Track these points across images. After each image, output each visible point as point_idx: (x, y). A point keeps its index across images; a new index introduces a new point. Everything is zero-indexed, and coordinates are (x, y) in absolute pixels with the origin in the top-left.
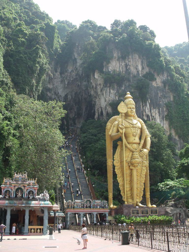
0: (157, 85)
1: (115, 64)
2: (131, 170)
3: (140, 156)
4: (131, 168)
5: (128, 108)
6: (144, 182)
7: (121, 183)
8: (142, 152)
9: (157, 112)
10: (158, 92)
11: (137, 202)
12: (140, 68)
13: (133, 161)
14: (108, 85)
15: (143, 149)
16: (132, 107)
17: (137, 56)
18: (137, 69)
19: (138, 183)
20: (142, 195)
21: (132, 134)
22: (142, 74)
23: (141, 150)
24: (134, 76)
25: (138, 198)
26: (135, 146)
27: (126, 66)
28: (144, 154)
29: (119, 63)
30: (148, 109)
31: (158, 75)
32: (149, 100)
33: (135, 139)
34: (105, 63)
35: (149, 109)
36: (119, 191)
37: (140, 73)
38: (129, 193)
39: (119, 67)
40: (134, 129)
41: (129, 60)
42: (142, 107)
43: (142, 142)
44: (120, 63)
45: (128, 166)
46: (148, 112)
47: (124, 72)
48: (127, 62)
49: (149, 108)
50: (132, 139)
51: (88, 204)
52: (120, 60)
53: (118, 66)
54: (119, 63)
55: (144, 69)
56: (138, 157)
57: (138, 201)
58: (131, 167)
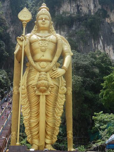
0: (111, 21)
2: (39, 96)
3: (51, 78)
4: (37, 94)
5: (39, 20)
6: (61, 114)
7: (26, 118)
9: (111, 48)
10: (112, 27)
11: (46, 144)
12: (92, 7)
14: (59, 27)
15: (56, 69)
16: (44, 17)
20: (57, 134)
21: (39, 50)
22: (94, 12)
23: (54, 69)
24: (85, 15)
25: (48, 137)
26: (44, 64)
27: (78, 6)
29: (71, 5)
30: (101, 46)
31: (111, 11)
32: (102, 37)
33: (45, 55)
34: (57, 8)
35: (102, 47)
36: (24, 128)
37: (92, 11)
38: (35, 129)
39: (71, 9)
41: (81, 1)
42: (93, 45)
43: (56, 58)
45: (34, 92)
47: (75, 13)
49: (102, 45)
50: (39, 56)
52: (72, 1)
53: (70, 8)
54: (71, 5)
55: (96, 7)
56: (46, 77)
58: (37, 93)
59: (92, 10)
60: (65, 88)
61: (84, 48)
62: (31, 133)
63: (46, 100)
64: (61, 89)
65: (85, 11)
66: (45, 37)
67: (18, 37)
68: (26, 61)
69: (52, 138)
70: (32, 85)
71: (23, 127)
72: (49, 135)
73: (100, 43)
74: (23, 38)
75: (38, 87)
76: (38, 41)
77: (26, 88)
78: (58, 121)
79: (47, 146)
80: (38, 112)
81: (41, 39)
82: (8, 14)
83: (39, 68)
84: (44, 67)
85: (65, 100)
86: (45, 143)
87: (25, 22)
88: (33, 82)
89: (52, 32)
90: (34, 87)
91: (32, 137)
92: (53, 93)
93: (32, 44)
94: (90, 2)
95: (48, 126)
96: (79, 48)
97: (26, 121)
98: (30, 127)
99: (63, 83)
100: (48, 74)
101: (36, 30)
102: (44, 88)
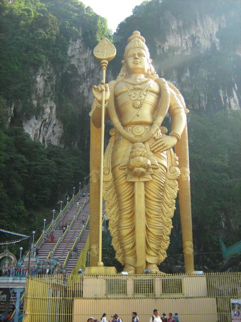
1: (174, 41)
2: (133, 183)
3: (153, 152)
5: (129, 57)
6: (172, 214)
8: (158, 141)
11: (147, 263)
13: (133, 162)
16: (136, 53)
17: (210, 19)
18: (211, 40)
19: (151, 216)
21: (131, 105)
28: (162, 147)
29: (181, 37)
30: (235, 101)
32: (236, 86)
34: (158, 43)
37: (217, 45)
38: (126, 240)
39: (182, 43)
40: (138, 92)
42: (222, 100)
43: (160, 119)
44: (183, 38)
46: (236, 107)
48: (194, 33)
49: (237, 100)
51: (7, 265)
52: (182, 32)
54: (181, 37)
57: (149, 261)
59: (216, 42)
60: (177, 169)
61: (206, 105)
62: (122, 245)
63: (145, 190)
64: (171, 171)
65: (205, 46)
66: (139, 85)
67: (95, 86)
68: (109, 126)
69: (158, 254)
70: (120, 165)
71: (107, 236)
72: (151, 250)
73: (233, 96)
74: (103, 87)
75: (130, 170)
76: (127, 91)
77: (111, 171)
78: (168, 225)
79: (150, 267)
80: (132, 210)
81: (133, 88)
82: (82, 60)
83: (132, 136)
84: (140, 134)
85: (178, 189)
86: (147, 262)
87: (105, 61)
88: (122, 160)
89: (152, 76)
90: (125, 169)
91: (124, 253)
92: (158, 179)
93: (118, 98)
94: (212, 30)
95: (150, 234)
96: (199, 105)
97: (113, 226)
98: (119, 237)
99: (173, 160)
100: (147, 145)
101: (125, 74)
102: (142, 169)
